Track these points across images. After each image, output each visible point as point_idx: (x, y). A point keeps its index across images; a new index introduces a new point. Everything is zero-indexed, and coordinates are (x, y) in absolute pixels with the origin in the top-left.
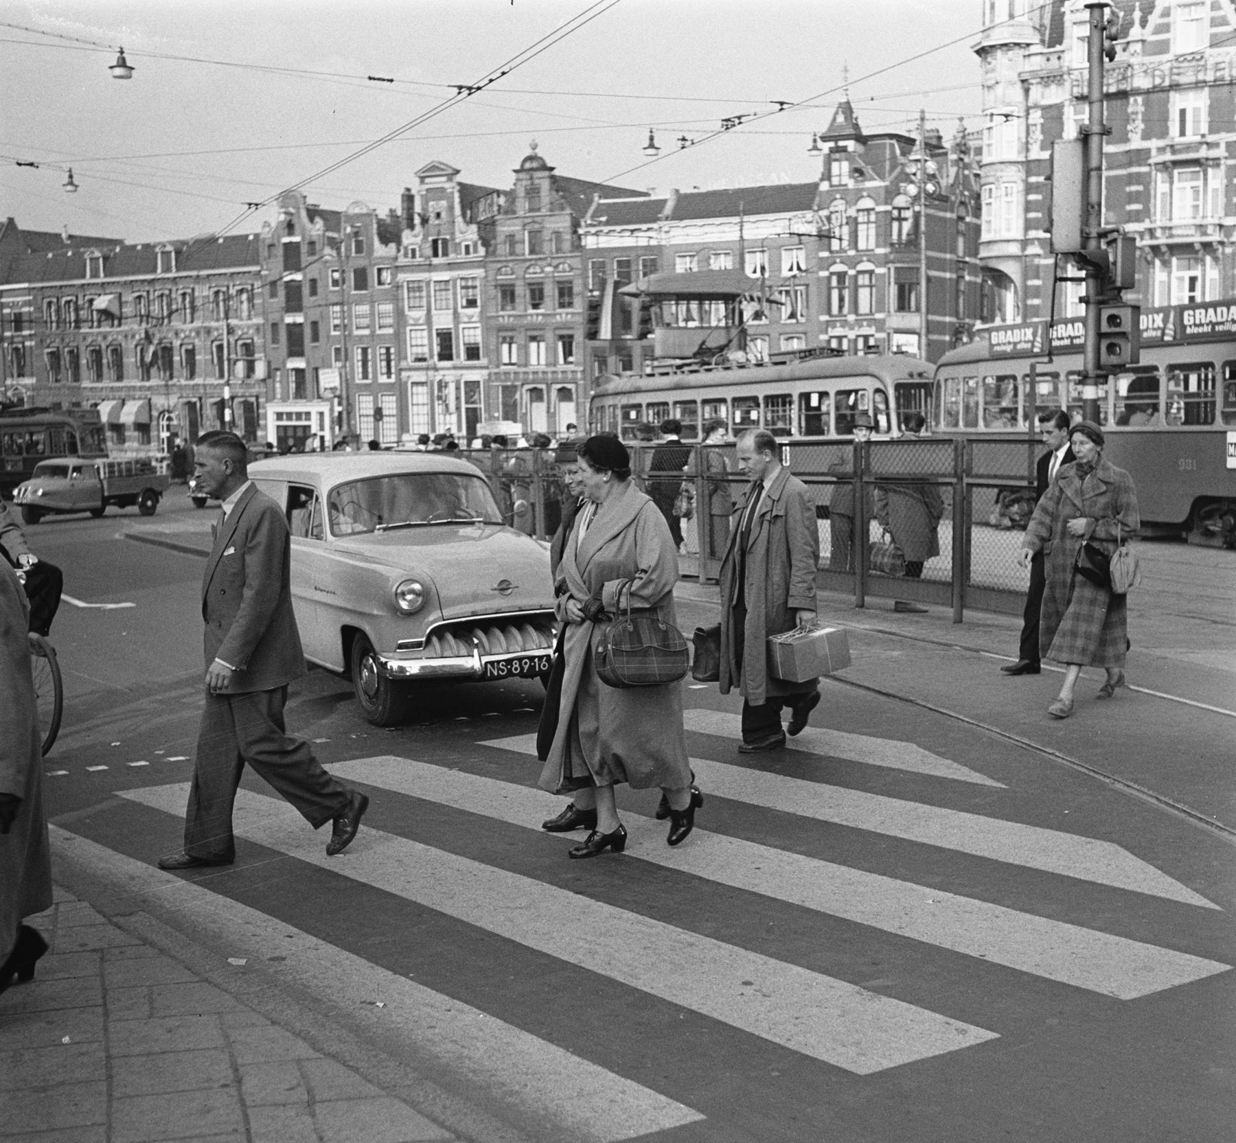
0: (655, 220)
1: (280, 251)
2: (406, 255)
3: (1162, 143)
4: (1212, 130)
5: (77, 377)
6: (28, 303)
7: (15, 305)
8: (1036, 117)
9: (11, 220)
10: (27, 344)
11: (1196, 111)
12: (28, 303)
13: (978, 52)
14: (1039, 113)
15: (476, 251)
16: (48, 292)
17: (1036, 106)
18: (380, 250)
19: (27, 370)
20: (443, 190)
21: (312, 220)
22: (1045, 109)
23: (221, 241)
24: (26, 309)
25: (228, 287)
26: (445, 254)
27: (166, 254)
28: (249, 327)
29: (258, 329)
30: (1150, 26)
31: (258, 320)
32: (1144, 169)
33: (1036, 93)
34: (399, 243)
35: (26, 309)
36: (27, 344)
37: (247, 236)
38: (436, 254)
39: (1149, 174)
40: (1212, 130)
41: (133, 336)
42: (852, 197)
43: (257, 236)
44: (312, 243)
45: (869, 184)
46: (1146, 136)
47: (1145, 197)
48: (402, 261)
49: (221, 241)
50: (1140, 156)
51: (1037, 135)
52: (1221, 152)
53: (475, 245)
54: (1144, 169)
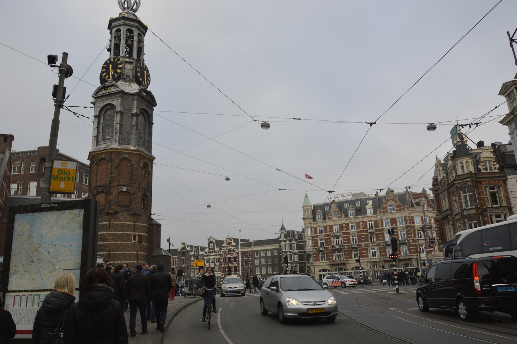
0: (251, 246)
1: (181, 253)
2: (205, 254)
3: (332, 233)
4: (340, 231)
8: (313, 229)
11: (337, 228)
13: (303, 219)
14: (313, 228)
15: (218, 252)
17: (313, 227)
18: (201, 253)
20: (212, 242)
21: (188, 247)
22: (314, 228)
26: (213, 253)
30: (329, 215)
31: (177, 266)
32: (330, 237)
33: (312, 225)
34: (204, 251)
38: (211, 253)
39: (331, 238)
40: (340, 231)
42: (285, 241)
44: (187, 252)
45: (288, 239)
46: (330, 232)
47: (331, 241)
48: (205, 254)
50: (329, 235)
51: (313, 232)
52: (341, 234)
53: (218, 251)
54: (330, 237)
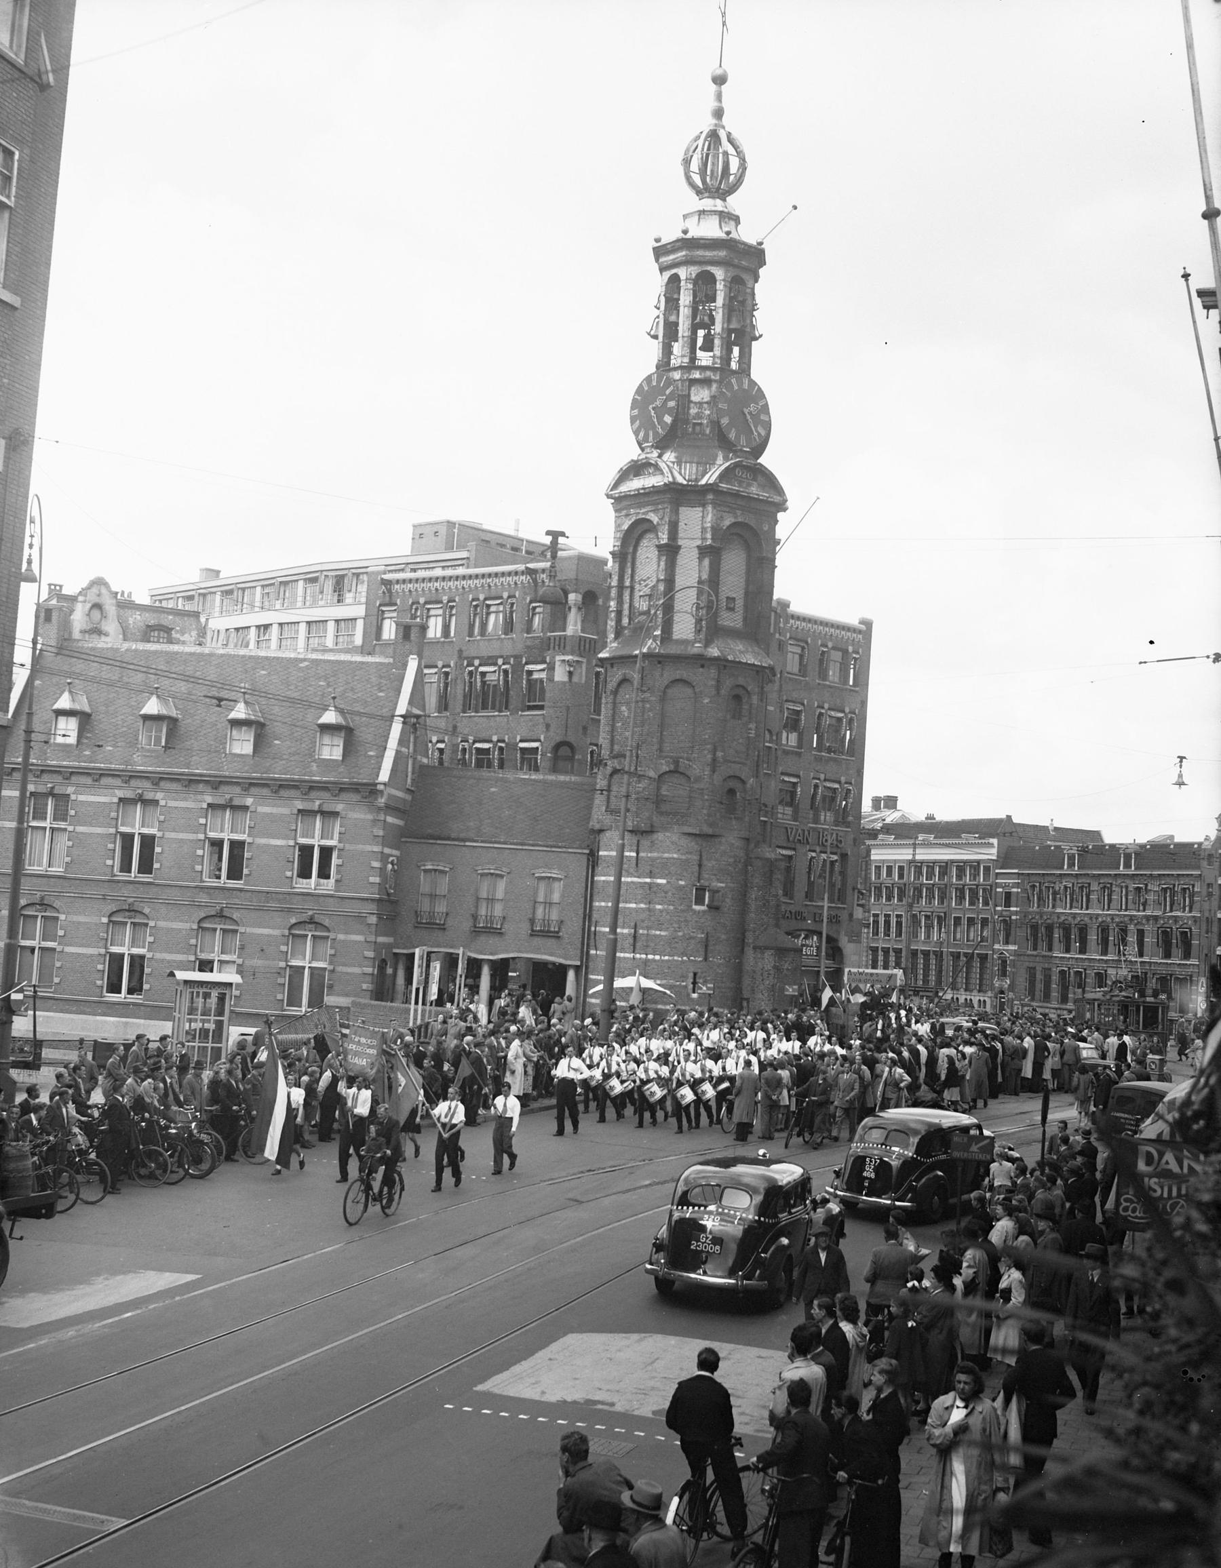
5: (1050, 949)
6: (1017, 885)
7: (1006, 885)
9: (1009, 817)
10: (1014, 917)
12: (1017, 885)
16: (1033, 878)
19: (1011, 939)
23: (1172, 847)
24: (1015, 890)
25: (1174, 885)
27: (1128, 857)
28: (1188, 918)
29: (1195, 919)
35: (1015, 890)
36: (1014, 917)
37: (1193, 844)
41: (1097, 918)
43: (1200, 844)
49: (1172, 847)
